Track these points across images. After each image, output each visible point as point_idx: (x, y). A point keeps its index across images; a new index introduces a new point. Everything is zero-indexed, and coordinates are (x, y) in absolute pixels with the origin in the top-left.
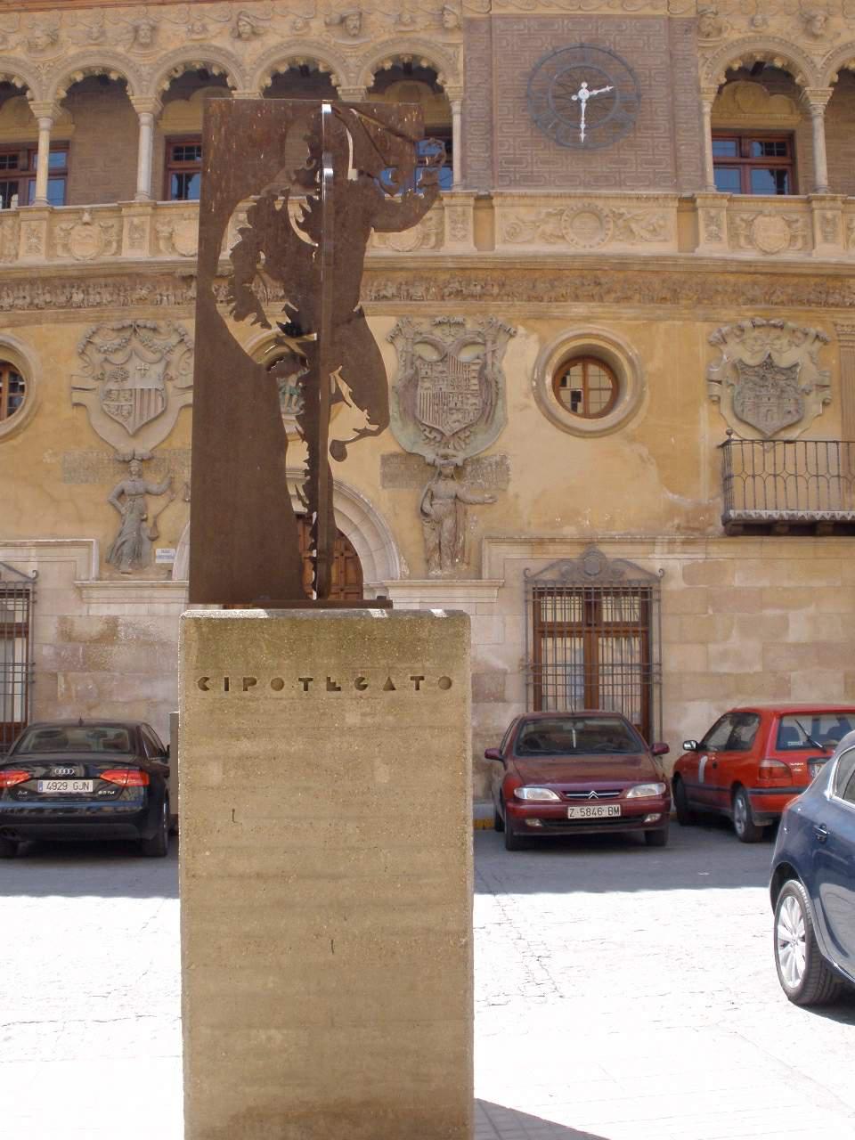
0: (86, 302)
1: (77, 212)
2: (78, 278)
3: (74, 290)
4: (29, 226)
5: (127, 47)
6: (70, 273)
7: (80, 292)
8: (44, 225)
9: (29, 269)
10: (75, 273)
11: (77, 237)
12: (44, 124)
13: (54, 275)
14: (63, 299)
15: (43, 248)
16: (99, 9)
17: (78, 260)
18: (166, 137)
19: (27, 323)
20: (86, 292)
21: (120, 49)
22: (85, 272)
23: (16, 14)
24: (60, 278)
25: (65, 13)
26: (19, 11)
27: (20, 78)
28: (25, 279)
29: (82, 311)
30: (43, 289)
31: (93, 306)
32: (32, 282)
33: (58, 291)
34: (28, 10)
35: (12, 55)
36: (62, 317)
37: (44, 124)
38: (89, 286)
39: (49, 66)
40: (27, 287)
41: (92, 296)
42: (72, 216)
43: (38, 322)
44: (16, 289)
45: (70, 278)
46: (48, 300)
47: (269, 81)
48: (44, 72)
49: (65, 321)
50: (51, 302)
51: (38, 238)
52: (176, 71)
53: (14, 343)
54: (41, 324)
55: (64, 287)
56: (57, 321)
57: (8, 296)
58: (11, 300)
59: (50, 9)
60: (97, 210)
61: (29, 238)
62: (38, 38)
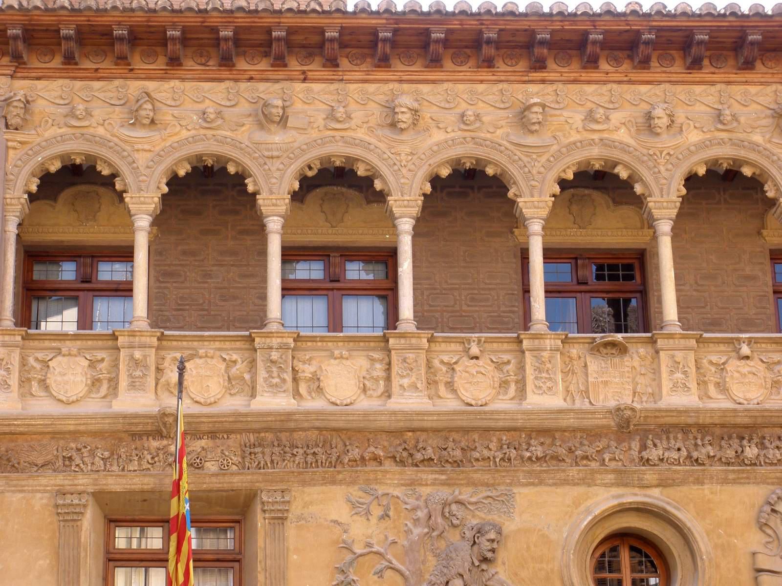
0: (762, 459)
1: (730, 341)
2: (746, 427)
3: (745, 442)
4: (673, 356)
5: (768, 136)
6: (739, 420)
7: (753, 446)
8: (691, 356)
9: (679, 412)
10: (746, 420)
11: (736, 375)
12: (536, 227)
13: (717, 422)
14: (730, 453)
15: (693, 386)
16: (723, 86)
17: (740, 404)
18: (771, 250)
19: (683, 482)
20: (762, 446)
21: (757, 138)
22: (759, 421)
23: (615, 86)
24: (723, 426)
25: (679, 88)
26: (620, 82)
27: (626, 166)
28: (675, 426)
29: (762, 470)
30: (702, 440)
31: (771, 464)
32: (685, 429)
33: (723, 443)
34: (630, 82)
35: (615, 136)
36: (731, 476)
37: (536, 227)
38: (764, 438)
39: (669, 154)
40: (680, 436)
41: (771, 451)
42: (722, 347)
43: (699, 482)
44: (664, 437)
45: (735, 426)
46: (712, 454)
47: (428, 188)
48: (662, 161)
49: (735, 482)
50: (714, 456)
51: (685, 373)
52: (310, 168)
53: (669, 508)
54: (703, 483)
55: (730, 438)
56: (725, 481)
57: (655, 445)
58: (661, 453)
59: (660, 82)
60: (757, 341)
61: (672, 372)
62: (659, 118)
